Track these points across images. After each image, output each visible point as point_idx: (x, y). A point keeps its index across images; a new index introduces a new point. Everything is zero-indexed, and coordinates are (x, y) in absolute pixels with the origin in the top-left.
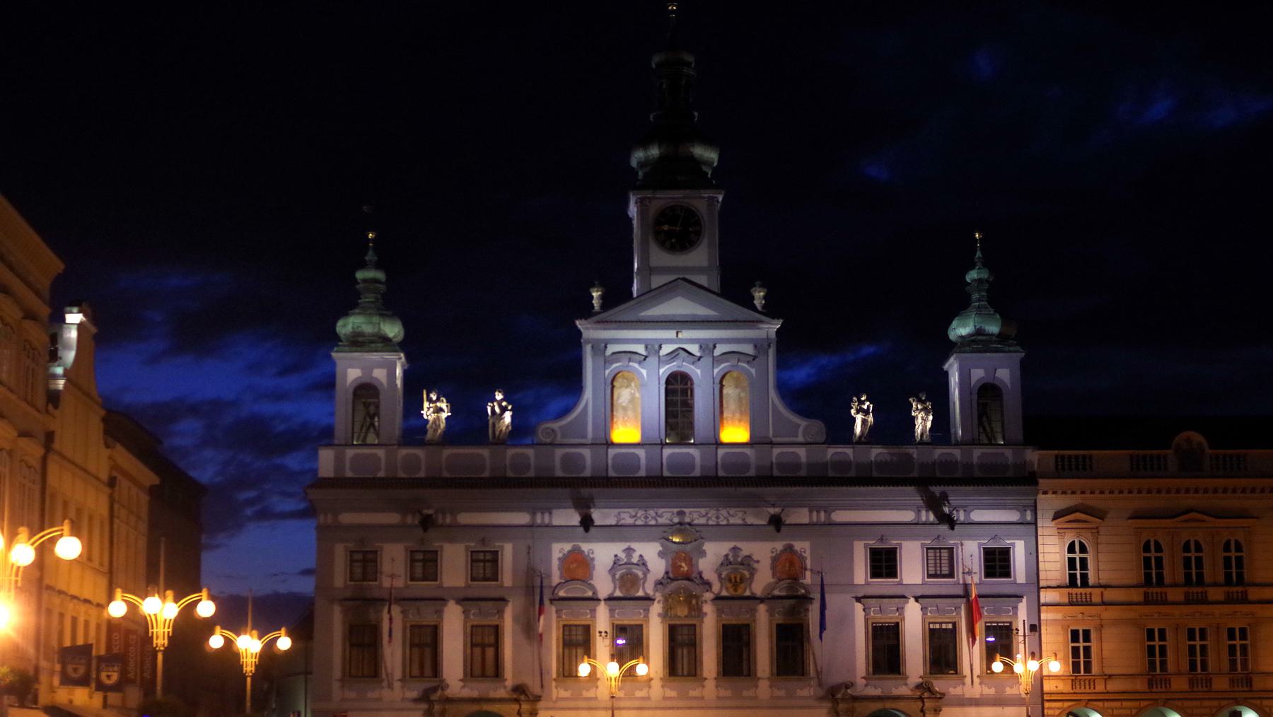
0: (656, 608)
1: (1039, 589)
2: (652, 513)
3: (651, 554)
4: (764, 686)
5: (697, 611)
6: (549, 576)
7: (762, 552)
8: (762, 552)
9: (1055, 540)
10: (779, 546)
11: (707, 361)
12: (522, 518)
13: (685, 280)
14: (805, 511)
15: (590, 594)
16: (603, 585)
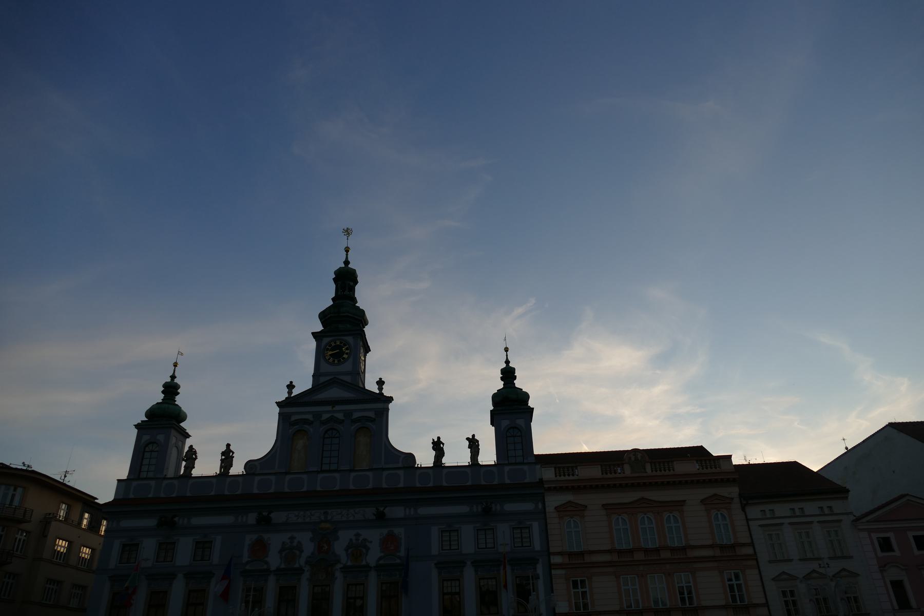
1: (549, 554)
7: (374, 536)
8: (374, 536)
10: (385, 531)
12: (228, 519)
15: (265, 567)
16: (274, 560)
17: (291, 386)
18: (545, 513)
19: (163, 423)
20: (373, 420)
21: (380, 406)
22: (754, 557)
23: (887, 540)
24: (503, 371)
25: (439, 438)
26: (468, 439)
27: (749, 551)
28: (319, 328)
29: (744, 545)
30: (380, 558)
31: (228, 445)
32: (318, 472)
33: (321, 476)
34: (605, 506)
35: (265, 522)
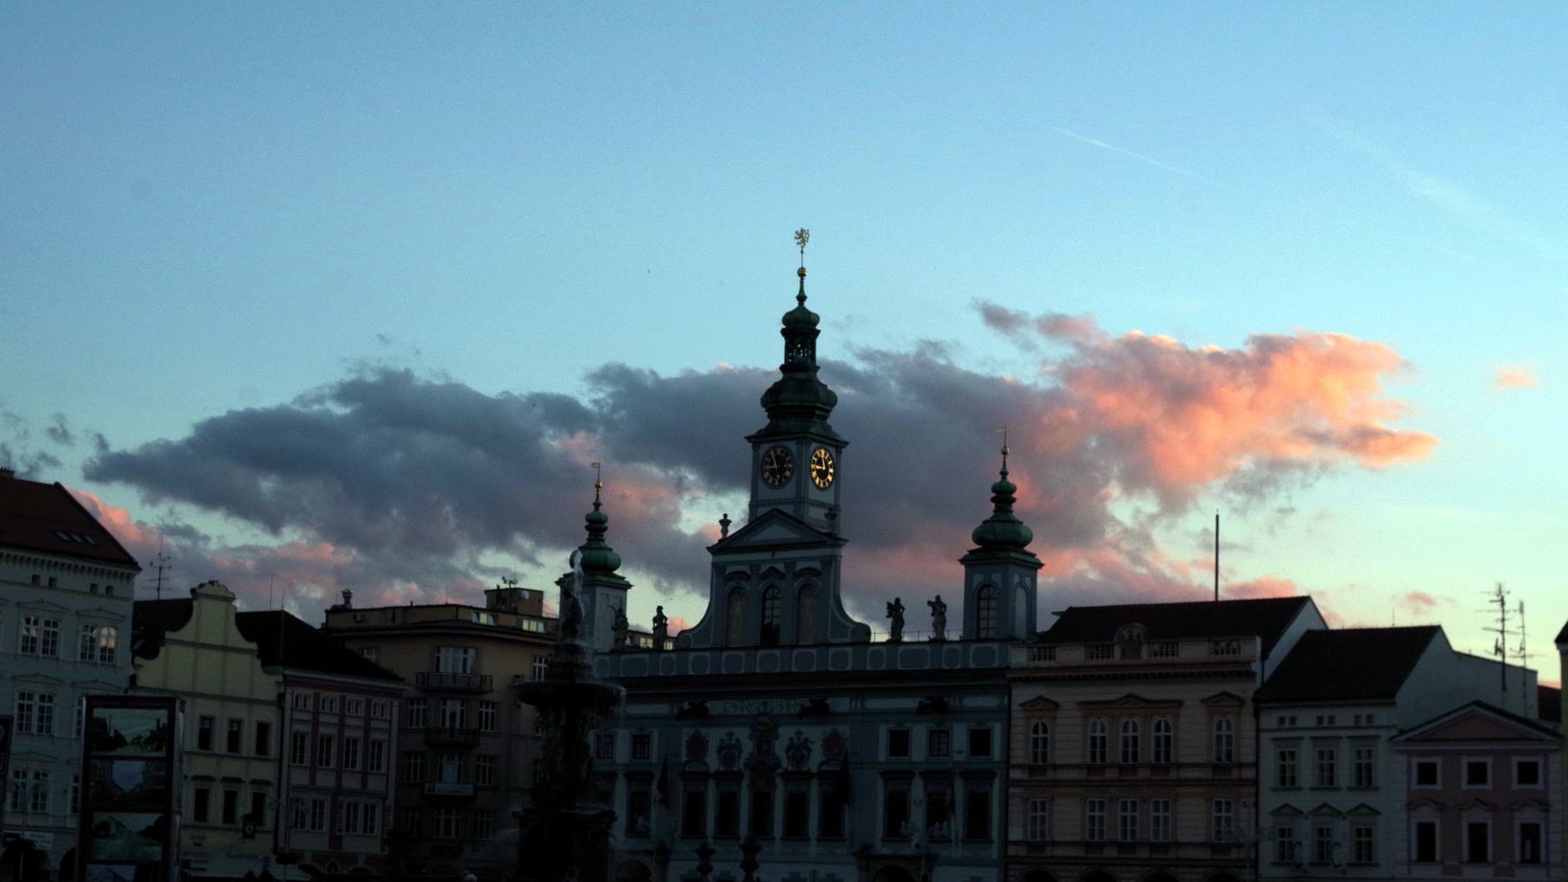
0: (745, 782)
3: (743, 734)
4: (813, 842)
8: (815, 734)
9: (1021, 722)
10: (828, 729)
12: (663, 709)
14: (847, 700)
16: (713, 762)
18: (1009, 711)
20: (819, 574)
21: (827, 551)
22: (1256, 782)
24: (996, 489)
25: (898, 600)
26: (930, 603)
27: (1249, 773)
28: (761, 420)
29: (1242, 765)
30: (822, 764)
31: (660, 609)
32: (757, 648)
33: (760, 653)
34: (1087, 707)
35: (699, 713)
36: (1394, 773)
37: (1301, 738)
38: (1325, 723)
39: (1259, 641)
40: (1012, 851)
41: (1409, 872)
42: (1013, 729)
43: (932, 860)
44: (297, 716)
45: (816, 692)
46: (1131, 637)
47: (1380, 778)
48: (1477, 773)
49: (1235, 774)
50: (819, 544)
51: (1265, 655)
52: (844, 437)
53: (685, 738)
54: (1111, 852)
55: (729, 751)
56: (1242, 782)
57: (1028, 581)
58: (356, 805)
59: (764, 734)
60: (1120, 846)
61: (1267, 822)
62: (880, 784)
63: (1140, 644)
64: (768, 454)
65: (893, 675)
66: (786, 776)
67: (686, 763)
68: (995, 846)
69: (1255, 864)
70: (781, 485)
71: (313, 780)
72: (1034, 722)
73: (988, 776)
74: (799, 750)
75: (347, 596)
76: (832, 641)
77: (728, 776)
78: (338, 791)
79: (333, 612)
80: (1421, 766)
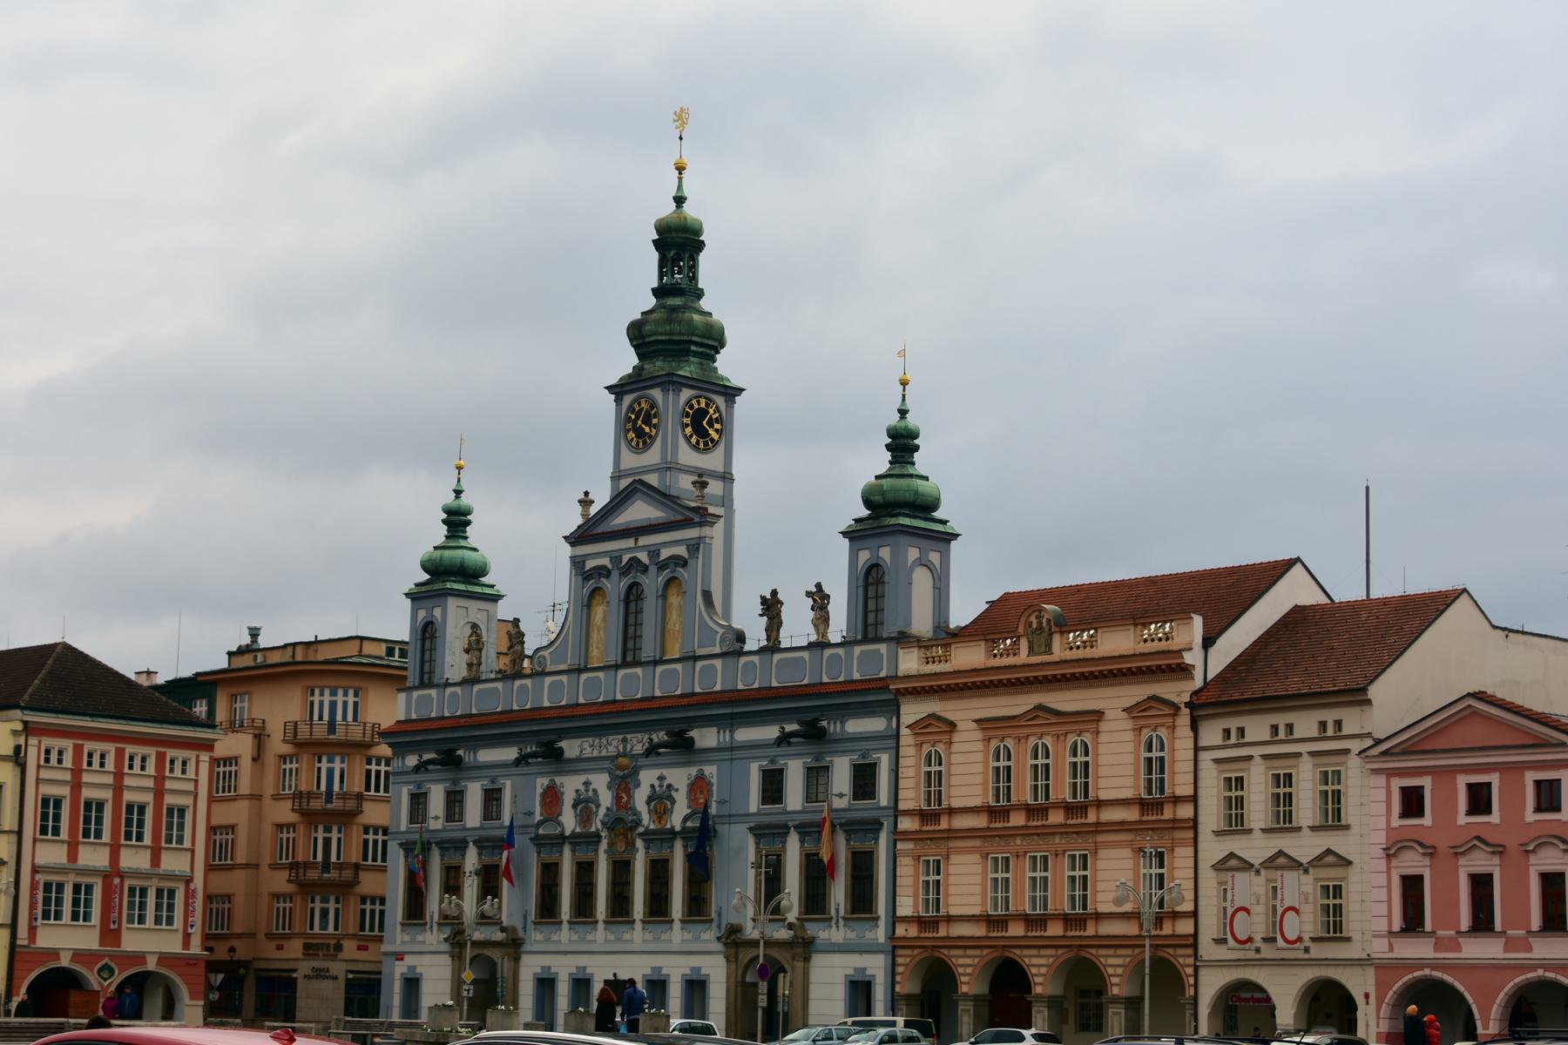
0: (604, 845)
1: (897, 813)
2: (604, 741)
3: (600, 781)
5: (631, 845)
6: (530, 814)
8: (679, 778)
9: (911, 751)
10: (693, 771)
11: (653, 569)
13: (641, 482)
14: (714, 730)
16: (569, 821)
17: (586, 502)
19: (451, 576)
22: (1194, 823)
23: (1419, 790)
25: (774, 593)
26: (809, 594)
27: (1185, 811)
29: (1176, 800)
30: (686, 819)
32: (617, 667)
33: (621, 673)
34: (986, 724)
35: (552, 755)
36: (1370, 803)
37: (1251, 757)
38: (1282, 735)
39: (1198, 621)
40: (900, 931)
41: (1391, 949)
42: (902, 762)
43: (804, 947)
44: (44, 774)
45: (673, 726)
46: (1040, 627)
47: (1350, 813)
48: (1479, 800)
49: (1168, 814)
50: (686, 523)
51: (1208, 642)
52: (735, 382)
53: (539, 791)
54: (1016, 930)
55: (584, 805)
56: (1175, 824)
57: (934, 557)
58: (60, 887)
59: (623, 783)
60: (1029, 921)
61: (1208, 879)
62: (751, 840)
63: (1051, 634)
64: (631, 409)
65: (768, 694)
66: (649, 837)
67: (540, 824)
68: (882, 923)
69: (1193, 941)
70: (647, 447)
71: (73, 855)
72: (926, 748)
73: (874, 827)
74: (661, 800)
75: (254, 633)
76: (700, 652)
77: (585, 840)
78: (113, 874)
79: (241, 651)
80: (1405, 791)
